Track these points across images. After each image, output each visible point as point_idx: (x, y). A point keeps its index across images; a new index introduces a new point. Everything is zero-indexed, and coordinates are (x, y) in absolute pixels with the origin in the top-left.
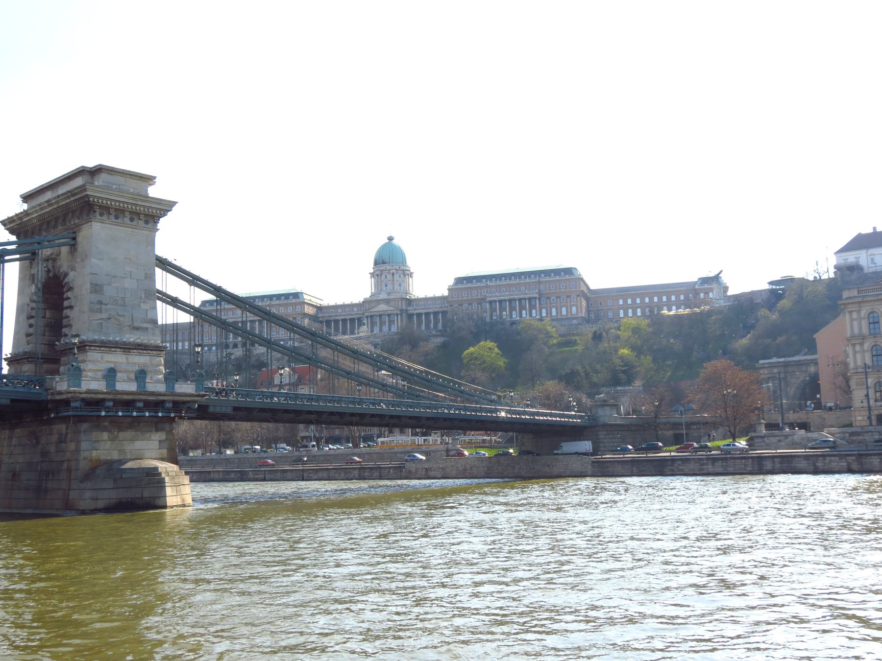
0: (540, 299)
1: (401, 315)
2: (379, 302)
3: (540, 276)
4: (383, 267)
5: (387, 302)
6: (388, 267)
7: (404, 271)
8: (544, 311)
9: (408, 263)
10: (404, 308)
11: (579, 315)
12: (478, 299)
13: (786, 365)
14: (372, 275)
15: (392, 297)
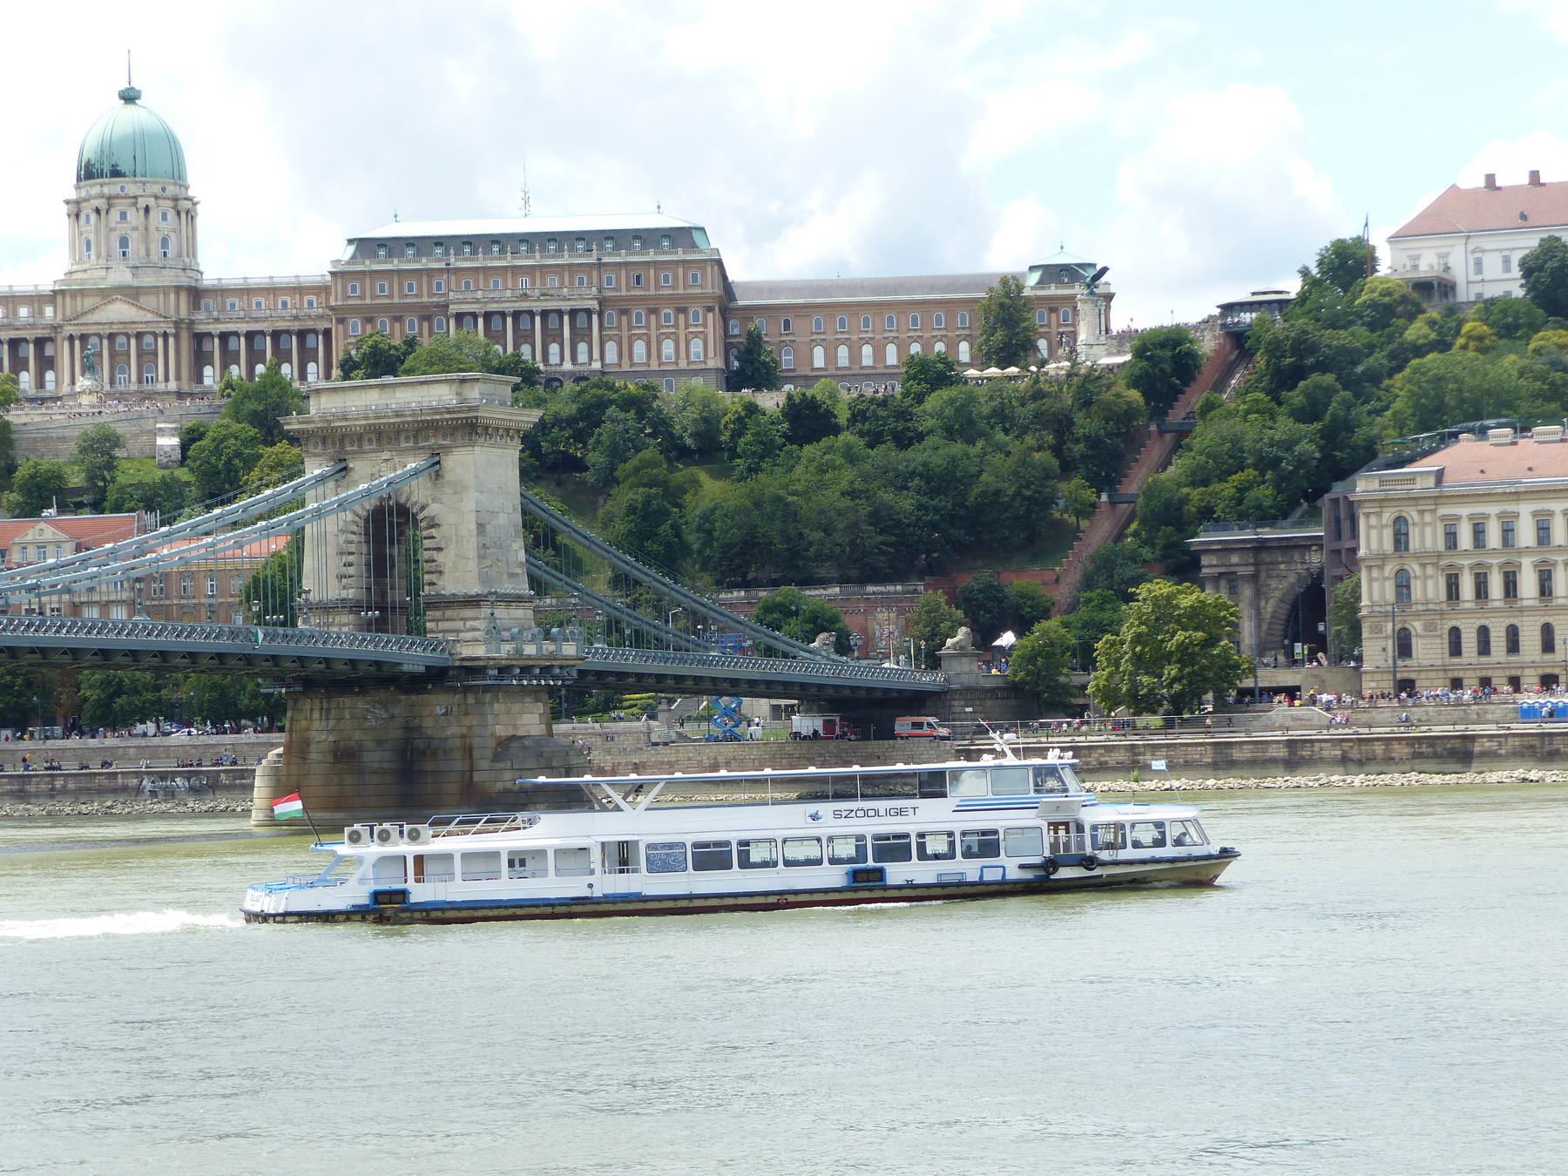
0: (600, 315)
1: (177, 336)
2: (107, 294)
3: (601, 247)
4: (112, 187)
5: (132, 294)
6: (132, 189)
7: (176, 199)
8: (611, 348)
9: (191, 178)
10: (184, 313)
11: (711, 364)
12: (422, 306)
13: (1261, 546)
14: (76, 211)
15: (148, 280)
